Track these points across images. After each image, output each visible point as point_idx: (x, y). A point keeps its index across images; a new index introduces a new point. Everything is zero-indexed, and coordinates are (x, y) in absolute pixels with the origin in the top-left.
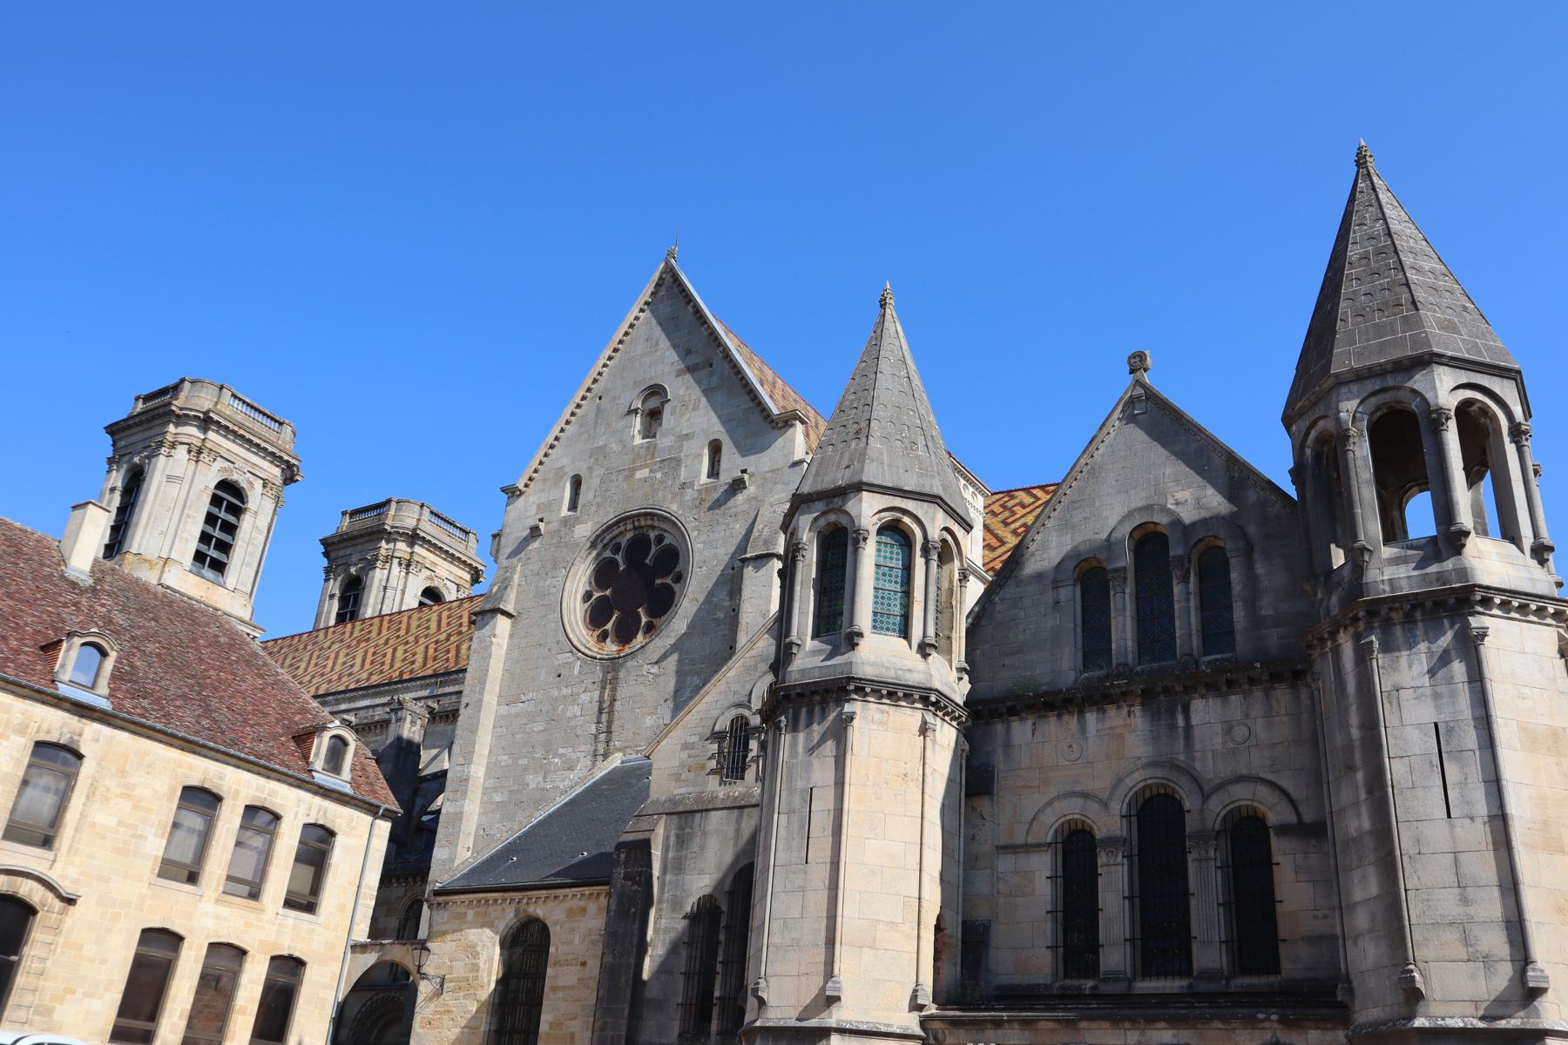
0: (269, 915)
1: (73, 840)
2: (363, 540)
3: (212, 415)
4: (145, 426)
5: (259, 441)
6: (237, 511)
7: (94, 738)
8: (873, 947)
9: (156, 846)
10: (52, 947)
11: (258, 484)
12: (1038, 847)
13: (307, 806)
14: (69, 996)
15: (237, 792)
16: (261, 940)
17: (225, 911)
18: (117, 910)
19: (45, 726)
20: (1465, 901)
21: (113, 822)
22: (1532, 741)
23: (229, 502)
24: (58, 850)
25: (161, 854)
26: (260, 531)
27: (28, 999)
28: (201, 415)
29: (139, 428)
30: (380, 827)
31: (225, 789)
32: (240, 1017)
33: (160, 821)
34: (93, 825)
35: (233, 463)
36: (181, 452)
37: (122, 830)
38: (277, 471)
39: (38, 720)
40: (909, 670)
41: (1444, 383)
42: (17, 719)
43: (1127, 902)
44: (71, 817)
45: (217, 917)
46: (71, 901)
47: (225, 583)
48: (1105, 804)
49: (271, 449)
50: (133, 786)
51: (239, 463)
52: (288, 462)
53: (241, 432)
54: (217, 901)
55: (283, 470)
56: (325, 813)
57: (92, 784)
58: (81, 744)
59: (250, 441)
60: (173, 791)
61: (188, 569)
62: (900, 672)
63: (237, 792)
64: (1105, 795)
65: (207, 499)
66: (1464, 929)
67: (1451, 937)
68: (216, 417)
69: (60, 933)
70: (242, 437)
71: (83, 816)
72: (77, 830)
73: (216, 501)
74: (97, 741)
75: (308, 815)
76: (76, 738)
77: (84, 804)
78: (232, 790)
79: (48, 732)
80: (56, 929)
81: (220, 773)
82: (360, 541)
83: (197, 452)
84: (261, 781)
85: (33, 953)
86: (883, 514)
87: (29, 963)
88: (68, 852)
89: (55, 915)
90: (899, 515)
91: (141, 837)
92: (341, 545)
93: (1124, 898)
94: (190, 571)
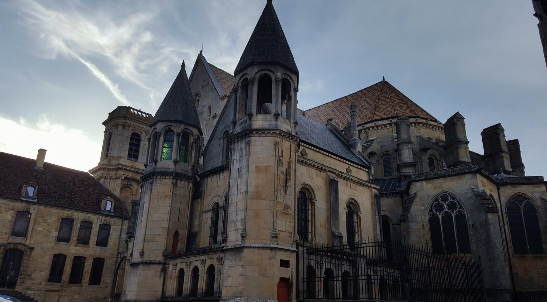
0: (91, 248)
1: (31, 234)
3: (126, 115)
5: (141, 121)
7: (33, 209)
8: (153, 241)
9: (55, 234)
10: (29, 260)
11: (144, 133)
12: (208, 211)
13: (100, 220)
14: (35, 272)
15: (78, 218)
16: (90, 255)
17: (78, 248)
18: (46, 250)
19: (19, 208)
20: (236, 215)
21: (42, 229)
22: (258, 169)
23: (136, 139)
24: (27, 237)
25: (57, 236)
26: (146, 145)
27: (24, 273)
29: (109, 122)
30: (125, 222)
31: (74, 218)
32: (86, 274)
33: (56, 228)
34: (37, 230)
35: (135, 128)
37: (45, 231)
39: (17, 206)
40: (169, 169)
41: (254, 71)
42: (11, 206)
43: (223, 223)
44: (30, 229)
45: (75, 250)
46: (32, 249)
47: (138, 161)
48: (221, 198)
50: (47, 220)
54: (75, 246)
56: (106, 221)
57: (34, 221)
58: (30, 211)
60: (58, 220)
61: (126, 158)
62: (166, 169)
63: (78, 218)
64: (221, 195)
65: (129, 139)
66: (235, 222)
67: (233, 225)
68: (127, 116)
69: (31, 256)
71: (33, 228)
72: (32, 232)
73: (132, 139)
74: (35, 210)
75: (101, 222)
76: (28, 209)
77: (33, 225)
78: (76, 218)
79: (20, 209)
80: (30, 256)
81: (72, 214)
83: (124, 126)
84: (86, 215)
85: (24, 262)
86: (166, 128)
87: (23, 264)
88: (30, 238)
89: (28, 253)
90: (170, 127)
91: (51, 232)
93: (222, 222)
94: (127, 159)
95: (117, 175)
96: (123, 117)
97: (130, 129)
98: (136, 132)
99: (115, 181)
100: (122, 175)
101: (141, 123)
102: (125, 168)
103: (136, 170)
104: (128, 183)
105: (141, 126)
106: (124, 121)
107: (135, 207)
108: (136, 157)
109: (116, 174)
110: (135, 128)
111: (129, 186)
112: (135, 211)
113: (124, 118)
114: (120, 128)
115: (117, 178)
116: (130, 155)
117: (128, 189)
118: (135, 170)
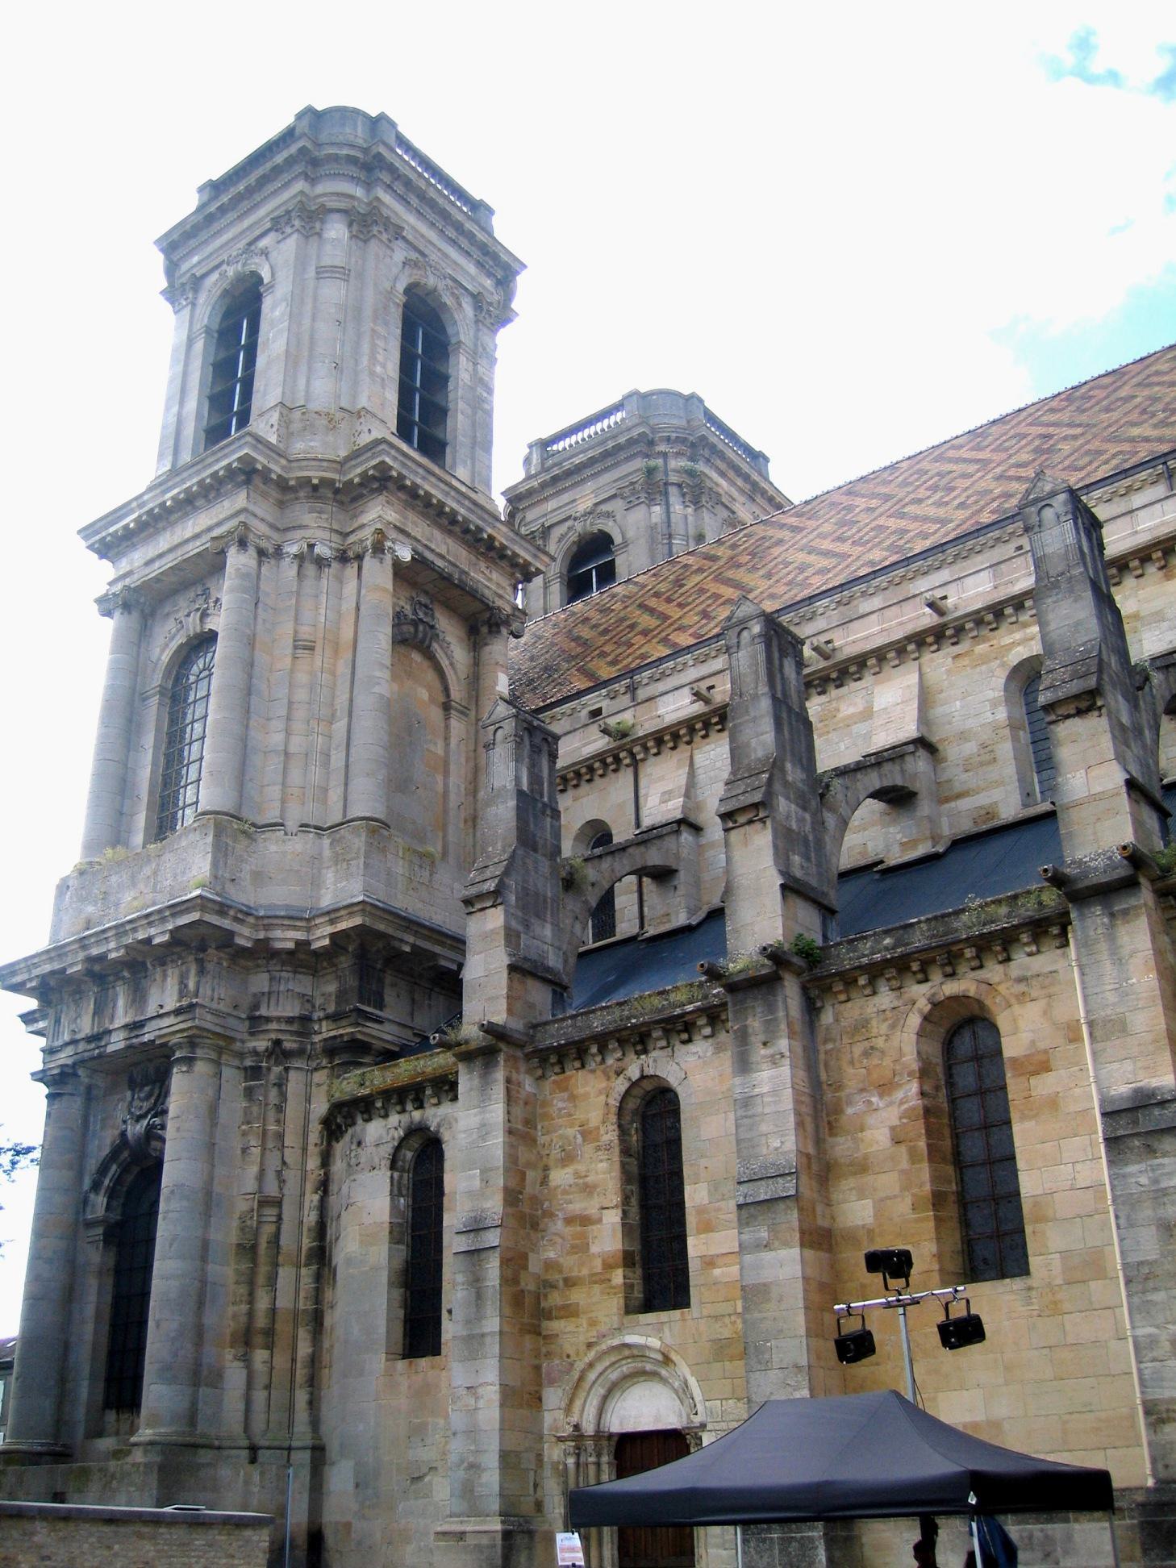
2: (598, 467)
4: (245, 205)
28: (359, 155)
51: (434, 256)
82: (588, 472)
92: (550, 491)
95: (346, 535)
97: (400, 253)
98: (431, 281)
99: (340, 581)
101: (451, 233)
102: (419, 481)
104: (421, 615)
105: (453, 253)
106: (359, 192)
107: (781, 666)
109: (335, 527)
111: (425, 635)
113: (363, 175)
114: (336, 230)
115: (359, 558)
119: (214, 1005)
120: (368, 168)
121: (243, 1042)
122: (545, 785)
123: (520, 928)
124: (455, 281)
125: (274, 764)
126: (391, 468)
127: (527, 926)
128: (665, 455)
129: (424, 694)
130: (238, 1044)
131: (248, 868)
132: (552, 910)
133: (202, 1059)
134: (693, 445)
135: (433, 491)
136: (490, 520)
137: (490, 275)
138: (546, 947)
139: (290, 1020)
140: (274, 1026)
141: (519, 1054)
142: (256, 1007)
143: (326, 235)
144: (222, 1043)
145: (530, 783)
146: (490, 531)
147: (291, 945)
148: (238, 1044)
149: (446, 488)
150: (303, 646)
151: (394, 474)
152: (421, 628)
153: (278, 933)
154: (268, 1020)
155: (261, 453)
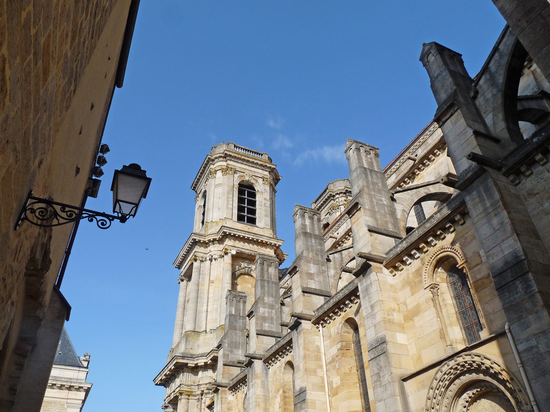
3: (226, 152)
5: (253, 160)
6: (253, 195)
11: (260, 181)
35: (244, 173)
36: (219, 174)
38: (267, 173)
49: (260, 163)
52: (270, 167)
53: (243, 157)
55: (270, 172)
59: (248, 161)
68: (228, 153)
70: (244, 160)
73: (241, 192)
96: (221, 157)
97: (236, 176)
98: (247, 178)
100: (231, 248)
102: (235, 233)
103: (258, 238)
106: (224, 164)
107: (268, 269)
108: (252, 221)
110: (242, 174)
112: (268, 277)
116: (240, 218)
117: (247, 276)
118: (255, 238)
119: (187, 383)
120: (225, 157)
121: (195, 392)
122: (241, 311)
123: (229, 353)
124: (255, 176)
125: (204, 315)
126: (226, 232)
127: (232, 352)
128: (338, 198)
129: (250, 286)
130: (194, 393)
131: (197, 344)
132: (242, 345)
133: (183, 399)
134: (345, 193)
135: (240, 234)
136: (260, 236)
137: (266, 171)
138: (239, 357)
139: (206, 384)
140: (202, 386)
141: (227, 389)
142: (199, 382)
143: (216, 177)
144: (189, 394)
145: (235, 311)
146: (261, 239)
147: (203, 364)
148: (194, 393)
149: (244, 232)
150: (211, 282)
151: (227, 233)
152: (246, 269)
153: (199, 361)
154: (201, 385)
155: (197, 237)
